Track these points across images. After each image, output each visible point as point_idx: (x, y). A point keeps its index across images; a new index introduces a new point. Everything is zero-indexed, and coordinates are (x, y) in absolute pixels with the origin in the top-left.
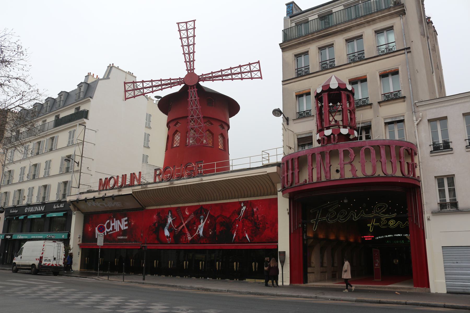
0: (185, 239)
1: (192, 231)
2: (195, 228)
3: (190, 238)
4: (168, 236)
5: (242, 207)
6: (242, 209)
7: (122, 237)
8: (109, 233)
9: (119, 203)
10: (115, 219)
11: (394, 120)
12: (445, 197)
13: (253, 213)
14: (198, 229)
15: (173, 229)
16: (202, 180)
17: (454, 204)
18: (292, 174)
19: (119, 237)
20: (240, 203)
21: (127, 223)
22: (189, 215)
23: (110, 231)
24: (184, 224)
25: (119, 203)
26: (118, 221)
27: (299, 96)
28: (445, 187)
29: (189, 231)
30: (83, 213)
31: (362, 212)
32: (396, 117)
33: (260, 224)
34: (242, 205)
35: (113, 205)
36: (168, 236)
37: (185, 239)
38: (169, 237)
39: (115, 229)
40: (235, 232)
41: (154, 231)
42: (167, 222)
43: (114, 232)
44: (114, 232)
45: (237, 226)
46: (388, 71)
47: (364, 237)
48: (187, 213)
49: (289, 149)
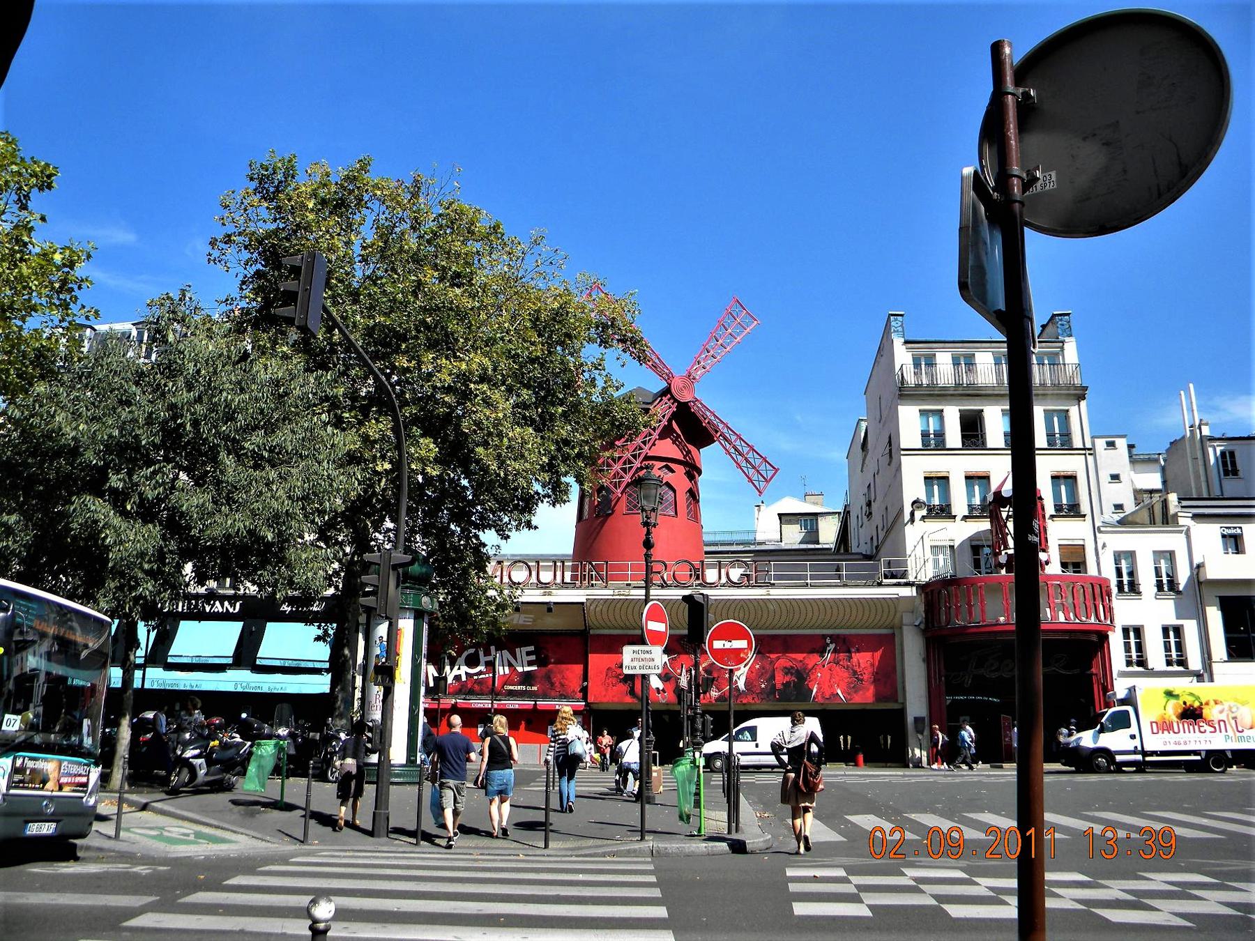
4: (661, 688)
5: (828, 645)
6: (828, 649)
7: (519, 688)
8: (475, 677)
10: (493, 648)
16: (769, 595)
17: (1142, 662)
19: (511, 688)
20: (824, 637)
21: (533, 658)
23: (480, 673)
26: (505, 652)
27: (929, 480)
28: (1163, 643)
34: (828, 641)
36: (661, 688)
38: (663, 690)
40: (816, 686)
45: (819, 675)
46: (1062, 474)
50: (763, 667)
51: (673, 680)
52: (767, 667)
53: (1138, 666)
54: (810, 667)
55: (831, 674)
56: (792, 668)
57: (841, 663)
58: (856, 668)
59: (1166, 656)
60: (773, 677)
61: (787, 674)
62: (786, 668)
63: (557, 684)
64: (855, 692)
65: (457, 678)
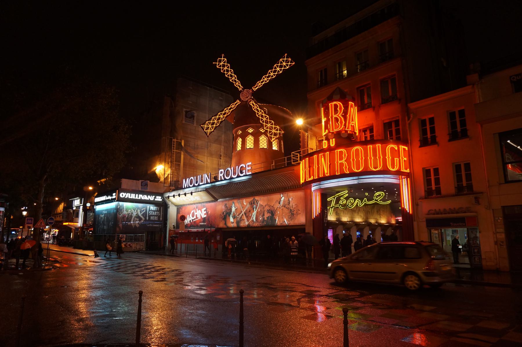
0: (244, 224)
1: (248, 217)
2: (250, 215)
3: (247, 223)
4: (233, 222)
6: (282, 200)
8: (194, 221)
9: (198, 198)
10: (197, 209)
11: (391, 120)
12: (431, 185)
13: (289, 203)
14: (253, 216)
15: (235, 216)
17: (438, 191)
18: (305, 171)
21: (205, 212)
22: (246, 205)
23: (194, 219)
24: (243, 213)
25: (198, 198)
26: (200, 211)
29: (247, 217)
30: (176, 206)
31: (365, 200)
32: (393, 118)
33: (294, 211)
34: (282, 196)
35: (195, 200)
36: (233, 222)
37: (244, 224)
38: (233, 222)
39: (198, 217)
40: (277, 218)
41: (223, 218)
42: (231, 211)
43: (197, 219)
44: (197, 219)
45: (279, 212)
47: (398, 218)
48: (245, 204)
49: (311, 150)
50: (261, 210)
51: (236, 218)
52: (262, 210)
53: (436, 195)
54: (276, 209)
55: (282, 212)
56: (270, 210)
57: (286, 206)
58: (291, 208)
59: (458, 185)
60: (264, 215)
61: (268, 213)
62: (268, 210)
63: (211, 222)
64: (291, 220)
65: (190, 221)
